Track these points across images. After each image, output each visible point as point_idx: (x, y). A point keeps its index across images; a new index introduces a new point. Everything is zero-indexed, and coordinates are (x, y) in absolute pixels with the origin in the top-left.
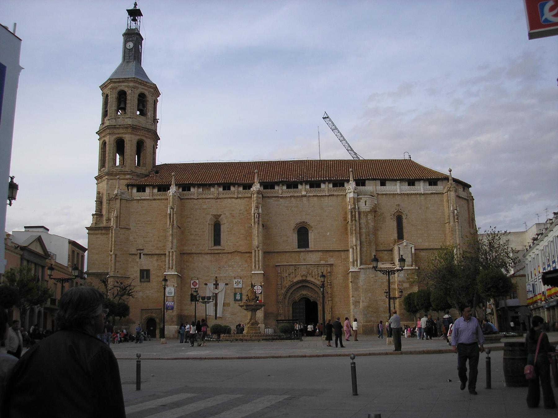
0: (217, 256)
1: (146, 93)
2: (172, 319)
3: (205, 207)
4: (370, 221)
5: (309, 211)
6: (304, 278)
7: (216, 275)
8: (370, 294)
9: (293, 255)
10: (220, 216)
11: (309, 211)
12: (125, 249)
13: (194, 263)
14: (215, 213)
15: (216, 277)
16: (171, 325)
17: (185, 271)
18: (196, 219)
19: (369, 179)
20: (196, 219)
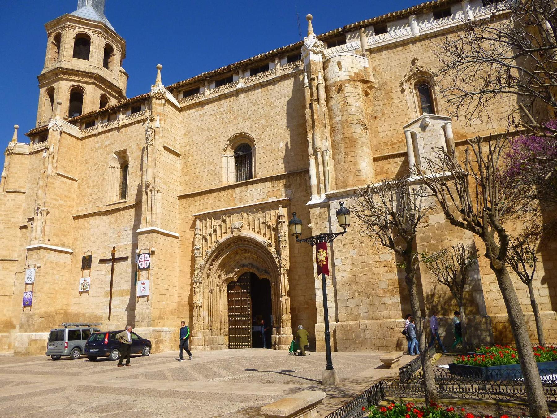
0: (117, 214)
1: (90, 33)
2: (28, 321)
3: (107, 143)
4: (350, 100)
5: (249, 113)
6: (236, 234)
7: (114, 245)
8: (354, 252)
9: (223, 193)
10: (125, 151)
11: (249, 113)
12: (13, 220)
13: (89, 230)
14: (118, 150)
15: (114, 248)
16: (26, 331)
17: (78, 242)
18: (97, 164)
19: (350, 31)
20: (97, 164)
